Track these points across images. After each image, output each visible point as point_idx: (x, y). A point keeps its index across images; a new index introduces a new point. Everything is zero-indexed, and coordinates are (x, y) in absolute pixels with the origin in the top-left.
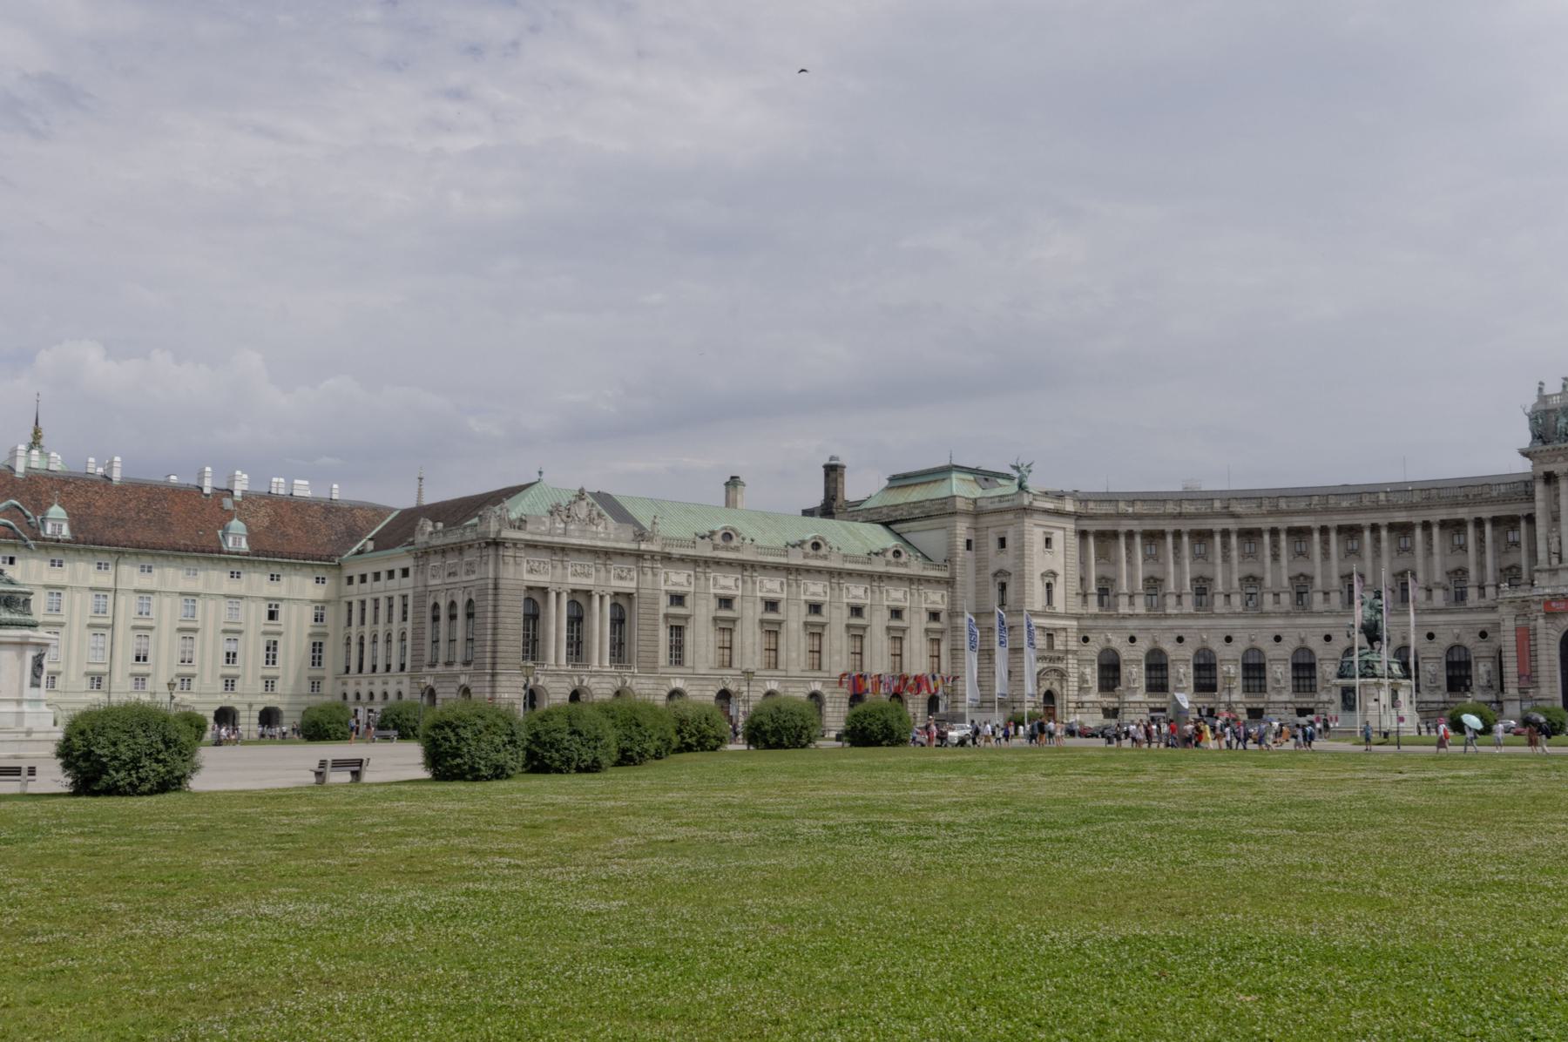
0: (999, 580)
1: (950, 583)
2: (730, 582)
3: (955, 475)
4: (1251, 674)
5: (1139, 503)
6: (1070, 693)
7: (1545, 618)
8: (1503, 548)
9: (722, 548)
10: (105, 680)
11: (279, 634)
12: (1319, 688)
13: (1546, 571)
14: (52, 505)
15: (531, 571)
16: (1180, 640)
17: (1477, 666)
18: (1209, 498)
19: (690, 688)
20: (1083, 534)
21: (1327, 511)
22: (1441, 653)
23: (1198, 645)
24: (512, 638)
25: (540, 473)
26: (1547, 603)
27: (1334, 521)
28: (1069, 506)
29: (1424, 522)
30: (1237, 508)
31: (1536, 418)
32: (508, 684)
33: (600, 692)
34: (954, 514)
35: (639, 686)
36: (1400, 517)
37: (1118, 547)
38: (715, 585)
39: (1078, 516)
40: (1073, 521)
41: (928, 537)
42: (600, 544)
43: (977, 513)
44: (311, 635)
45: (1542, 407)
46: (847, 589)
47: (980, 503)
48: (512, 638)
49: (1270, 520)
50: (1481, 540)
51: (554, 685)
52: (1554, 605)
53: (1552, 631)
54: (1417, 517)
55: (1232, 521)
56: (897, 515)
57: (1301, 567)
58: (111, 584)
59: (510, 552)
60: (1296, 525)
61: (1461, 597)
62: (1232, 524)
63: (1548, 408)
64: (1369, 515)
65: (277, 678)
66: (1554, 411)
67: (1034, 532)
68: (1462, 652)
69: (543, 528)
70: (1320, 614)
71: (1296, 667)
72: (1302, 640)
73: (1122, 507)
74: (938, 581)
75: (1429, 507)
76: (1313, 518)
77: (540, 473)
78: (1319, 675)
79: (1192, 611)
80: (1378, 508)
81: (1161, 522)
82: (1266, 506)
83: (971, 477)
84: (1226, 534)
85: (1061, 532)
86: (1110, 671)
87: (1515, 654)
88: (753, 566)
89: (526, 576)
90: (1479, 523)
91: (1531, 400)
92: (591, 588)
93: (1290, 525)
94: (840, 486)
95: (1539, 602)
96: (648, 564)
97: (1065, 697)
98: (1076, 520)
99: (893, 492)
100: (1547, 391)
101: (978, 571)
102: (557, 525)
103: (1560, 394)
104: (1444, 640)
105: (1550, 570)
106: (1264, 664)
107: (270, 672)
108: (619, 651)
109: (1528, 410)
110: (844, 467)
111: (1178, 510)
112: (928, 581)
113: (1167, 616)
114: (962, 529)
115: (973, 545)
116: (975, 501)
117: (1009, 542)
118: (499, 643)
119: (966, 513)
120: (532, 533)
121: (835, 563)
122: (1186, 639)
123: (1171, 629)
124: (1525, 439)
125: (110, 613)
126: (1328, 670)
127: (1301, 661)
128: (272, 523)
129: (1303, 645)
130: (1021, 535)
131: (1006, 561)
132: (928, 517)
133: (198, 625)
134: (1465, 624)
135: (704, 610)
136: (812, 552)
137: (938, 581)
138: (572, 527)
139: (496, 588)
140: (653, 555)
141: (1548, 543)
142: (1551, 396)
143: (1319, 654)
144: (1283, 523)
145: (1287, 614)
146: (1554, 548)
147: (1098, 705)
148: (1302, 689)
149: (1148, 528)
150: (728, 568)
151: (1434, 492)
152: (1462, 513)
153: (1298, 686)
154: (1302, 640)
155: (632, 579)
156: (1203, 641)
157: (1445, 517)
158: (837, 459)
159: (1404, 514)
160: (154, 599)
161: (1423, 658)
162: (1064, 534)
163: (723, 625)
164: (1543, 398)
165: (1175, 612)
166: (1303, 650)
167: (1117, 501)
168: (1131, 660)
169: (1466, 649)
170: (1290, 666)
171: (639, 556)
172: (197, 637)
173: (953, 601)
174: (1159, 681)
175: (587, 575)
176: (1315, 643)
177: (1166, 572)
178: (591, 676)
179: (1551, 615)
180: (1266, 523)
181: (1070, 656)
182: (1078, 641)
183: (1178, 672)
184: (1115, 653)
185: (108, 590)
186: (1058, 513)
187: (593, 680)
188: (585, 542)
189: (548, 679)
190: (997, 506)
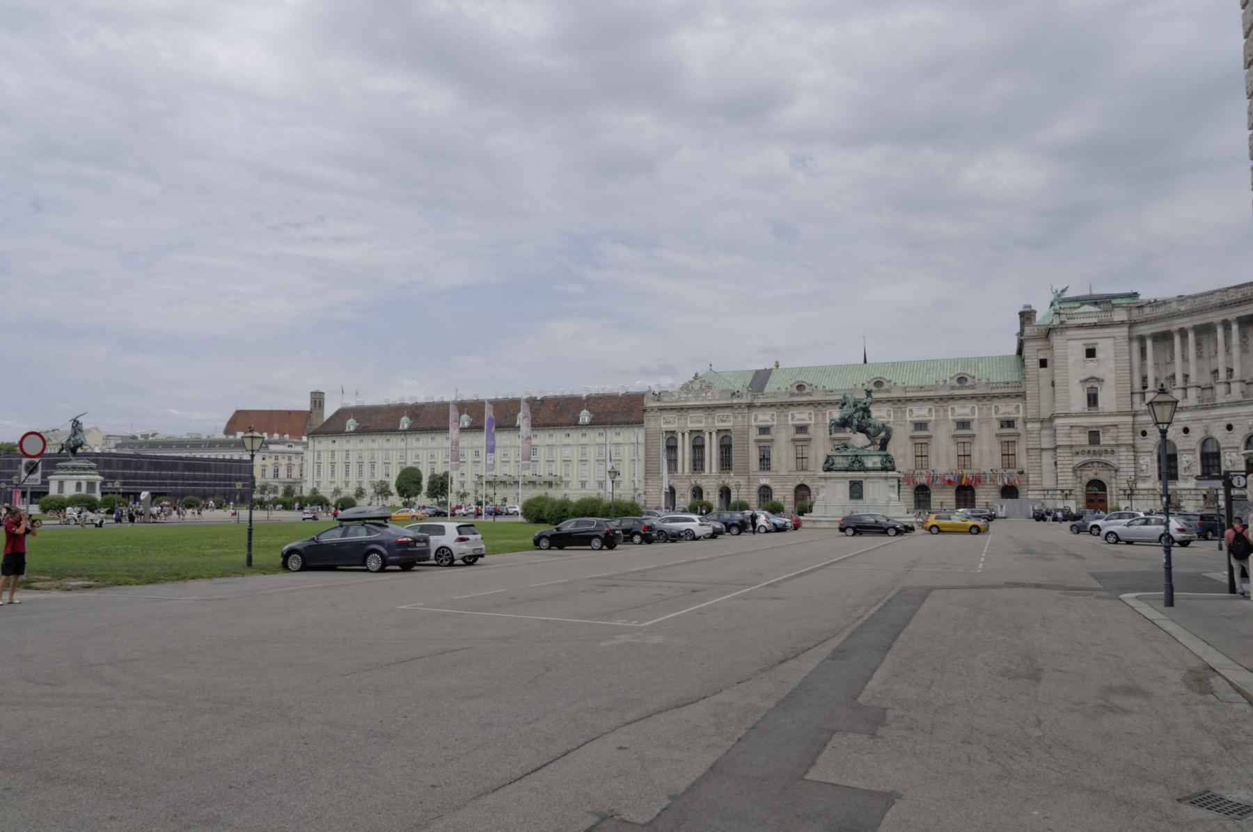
10: (604, 484)
15: (667, 423)
16: (1230, 427)
19: (774, 484)
24: (654, 459)
25: (711, 365)
38: (792, 419)
39: (1132, 324)
42: (707, 403)
46: (911, 410)
48: (654, 459)
51: (678, 484)
58: (604, 442)
69: (673, 398)
77: (711, 365)
81: (1210, 315)
85: (1110, 341)
92: (675, 429)
102: (682, 396)
108: (726, 463)
110: (1035, 312)
113: (1215, 406)
115: (1049, 363)
120: (666, 402)
122: (1235, 427)
123: (1221, 417)
125: (604, 455)
133: (588, 459)
138: (690, 396)
140: (739, 406)
149: (1198, 323)
158: (1030, 307)
160: (621, 447)
162: (1111, 346)
165: (1224, 401)
175: (701, 422)
178: (702, 479)
185: (603, 444)
187: (703, 481)
189: (676, 481)
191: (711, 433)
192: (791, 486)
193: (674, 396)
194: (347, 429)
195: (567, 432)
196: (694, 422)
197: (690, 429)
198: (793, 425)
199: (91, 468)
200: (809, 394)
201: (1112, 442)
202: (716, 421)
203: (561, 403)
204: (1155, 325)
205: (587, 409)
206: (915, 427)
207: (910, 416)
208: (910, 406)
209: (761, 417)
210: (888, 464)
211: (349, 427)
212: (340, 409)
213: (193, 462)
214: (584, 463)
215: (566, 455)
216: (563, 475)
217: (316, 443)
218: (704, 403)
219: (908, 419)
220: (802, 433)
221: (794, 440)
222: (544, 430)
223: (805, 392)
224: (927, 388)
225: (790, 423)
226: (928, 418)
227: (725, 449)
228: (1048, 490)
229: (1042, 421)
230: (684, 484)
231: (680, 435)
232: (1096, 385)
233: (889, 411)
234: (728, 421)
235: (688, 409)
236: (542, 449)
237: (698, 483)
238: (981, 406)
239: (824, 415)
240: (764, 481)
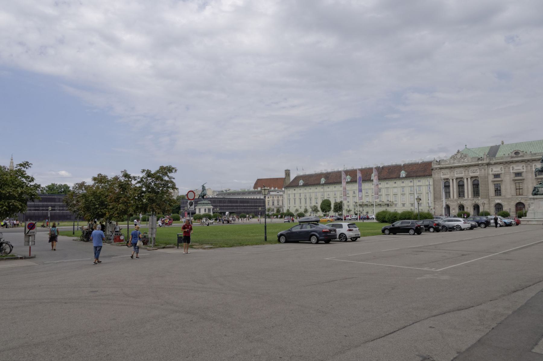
9: (515, 157)
15: (444, 175)
25: (466, 146)
32: (438, 204)
33: (467, 205)
38: (513, 170)
42: (465, 164)
48: (438, 192)
51: (451, 204)
58: (413, 185)
69: (447, 163)
77: (466, 146)
108: (476, 193)
120: (443, 165)
125: (413, 191)
133: (405, 193)
135: (508, 178)
138: (456, 161)
140: (482, 164)
160: (421, 188)
171: (478, 165)
178: (464, 201)
185: (412, 186)
187: (464, 202)
188: (459, 164)
189: (450, 202)
191: (467, 179)
192: (513, 203)
193: (447, 162)
194: (300, 185)
195: (395, 181)
196: (457, 174)
197: (456, 177)
198: (513, 173)
199: (209, 203)
202: (455, 174)
203: (391, 169)
205: (404, 170)
206: (494, 176)
209: (494, 169)
211: (301, 184)
212: (296, 176)
213: (231, 200)
214: (403, 195)
215: (395, 192)
216: (394, 201)
217: (288, 190)
218: (463, 164)
219: (512, 171)
220: (518, 176)
221: (514, 180)
223: (520, 155)
224: (537, 155)
225: (512, 171)
226: (501, 172)
227: (476, 186)
230: (454, 203)
231: (451, 181)
233: (502, 168)
234: (477, 172)
235: (455, 167)
236: (384, 190)
237: (462, 203)
238: (527, 165)
239: (531, 166)
240: (498, 201)
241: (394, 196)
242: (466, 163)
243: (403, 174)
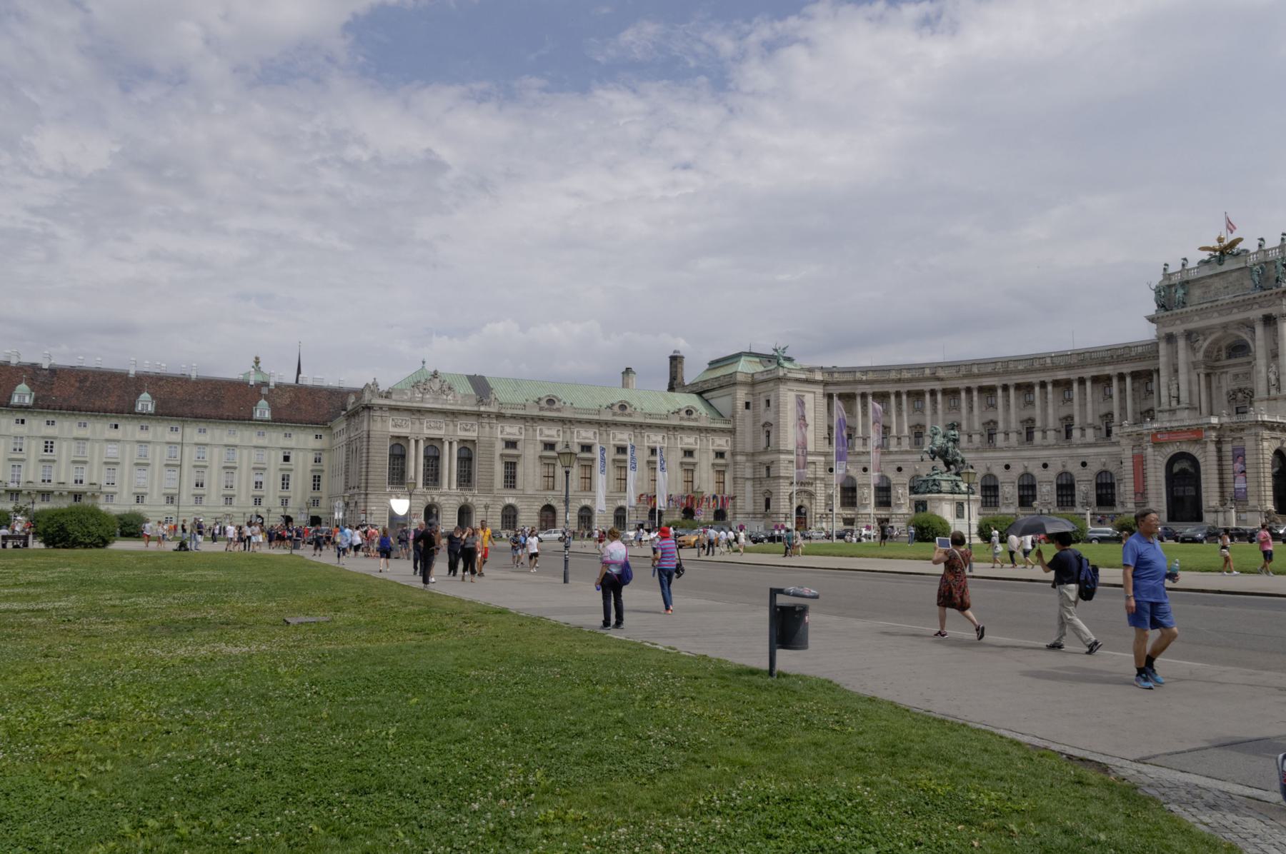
0: (766, 429)
1: (732, 432)
2: (691, 440)
3: (743, 358)
4: (988, 493)
5: (871, 373)
6: (819, 507)
7: (1153, 447)
8: (1143, 396)
10: (176, 498)
11: (291, 470)
12: (1000, 504)
13: (1166, 411)
14: (20, 382)
15: (395, 426)
16: (899, 469)
17: (1119, 486)
18: (921, 368)
19: (520, 504)
20: (830, 396)
21: (1007, 372)
22: (1092, 477)
23: (913, 473)
24: (379, 470)
25: (424, 362)
26: (1154, 435)
27: (1012, 380)
28: (819, 376)
29: (1079, 378)
30: (941, 373)
31: (1160, 291)
32: (376, 500)
33: (447, 506)
34: (735, 384)
35: (479, 502)
36: (1062, 375)
37: (856, 404)
38: (541, 435)
39: (825, 384)
40: (822, 387)
41: (721, 402)
42: (449, 407)
43: (753, 383)
44: (312, 471)
45: (1167, 283)
46: (648, 436)
47: (756, 376)
48: (379, 470)
49: (965, 381)
50: (1122, 391)
52: (1159, 436)
53: (1159, 458)
54: (1073, 375)
55: (938, 383)
56: (705, 387)
57: (990, 416)
58: (179, 440)
59: (378, 413)
60: (984, 384)
61: (1068, 434)
62: (937, 386)
63: (1171, 283)
64: (1039, 375)
65: (290, 497)
66: (1174, 285)
67: (788, 396)
68: (1109, 476)
70: (1001, 449)
71: (1060, 487)
72: (988, 469)
73: (858, 375)
74: (722, 431)
75: (1083, 367)
76: (996, 379)
77: (424, 362)
78: (1000, 494)
79: (908, 449)
80: (1044, 369)
81: (887, 386)
82: (963, 371)
83: (758, 360)
84: (933, 393)
85: (812, 395)
86: (849, 494)
87: (1132, 476)
88: (641, 426)
89: (391, 429)
90: (1121, 377)
91: (1157, 279)
93: (980, 385)
94: (679, 370)
95: (1148, 435)
96: (486, 420)
97: (813, 510)
98: (824, 386)
99: (709, 372)
100: (1170, 271)
101: (754, 423)
103: (1180, 272)
104: (1094, 467)
105: (1170, 410)
106: (997, 486)
107: (285, 494)
108: (466, 479)
109: (1154, 287)
110: (683, 357)
111: (899, 376)
112: (714, 430)
113: (890, 453)
114: (741, 395)
115: (751, 406)
116: (753, 375)
117: (771, 403)
118: (369, 474)
119: (744, 384)
120: (396, 401)
121: (638, 419)
122: (904, 469)
123: (893, 462)
124: (1152, 308)
125: (179, 458)
126: (1007, 490)
127: (988, 484)
128: (291, 402)
129: (989, 472)
130: (778, 397)
131: (769, 416)
132: (721, 387)
134: (1109, 454)
135: (532, 451)
136: (619, 412)
137: (722, 431)
138: (428, 396)
139: (369, 437)
140: (489, 415)
141: (1169, 389)
142: (1173, 274)
143: (1001, 478)
144: (973, 384)
145: (977, 450)
146: (1174, 393)
147: (840, 516)
148: (989, 504)
149: (876, 390)
150: (551, 423)
151: (1087, 355)
152: (1108, 370)
153: (986, 502)
154: (988, 469)
155: (474, 431)
156: (916, 470)
157: (1095, 374)
158: (679, 352)
159: (1065, 372)
161: (1078, 481)
162: (814, 400)
163: (586, 463)
164: (1167, 276)
165: (896, 449)
166: (1026, 475)
167: (855, 372)
168: (864, 484)
169: (1111, 474)
170: (1055, 486)
171: (479, 415)
172: (236, 472)
173: (734, 444)
174: (885, 499)
175: (440, 428)
176: (998, 471)
177: (891, 422)
179: (1157, 444)
180: (962, 384)
181: (818, 482)
182: (825, 471)
183: (897, 492)
184: (853, 479)
185: (178, 443)
186: (807, 381)
190: (765, 377)
192: (538, 506)
193: (406, 394)
195: (114, 421)
196: (429, 428)
198: (541, 441)
200: (558, 410)
201: (812, 476)
203: (91, 379)
204: (842, 387)
207: (648, 442)
208: (612, 431)
209: (508, 429)
210: (957, 489)
214: (259, 472)
215: (109, 455)
216: (104, 483)
218: (444, 407)
222: (163, 420)
223: (555, 407)
225: (538, 438)
227: (466, 459)
228: (749, 514)
229: (747, 455)
230: (419, 501)
231: (413, 442)
232: (769, 429)
234: (470, 431)
236: (65, 444)
237: (436, 500)
239: (535, 431)
240: (510, 501)
241: (105, 468)
242: (451, 404)
243: (145, 402)
